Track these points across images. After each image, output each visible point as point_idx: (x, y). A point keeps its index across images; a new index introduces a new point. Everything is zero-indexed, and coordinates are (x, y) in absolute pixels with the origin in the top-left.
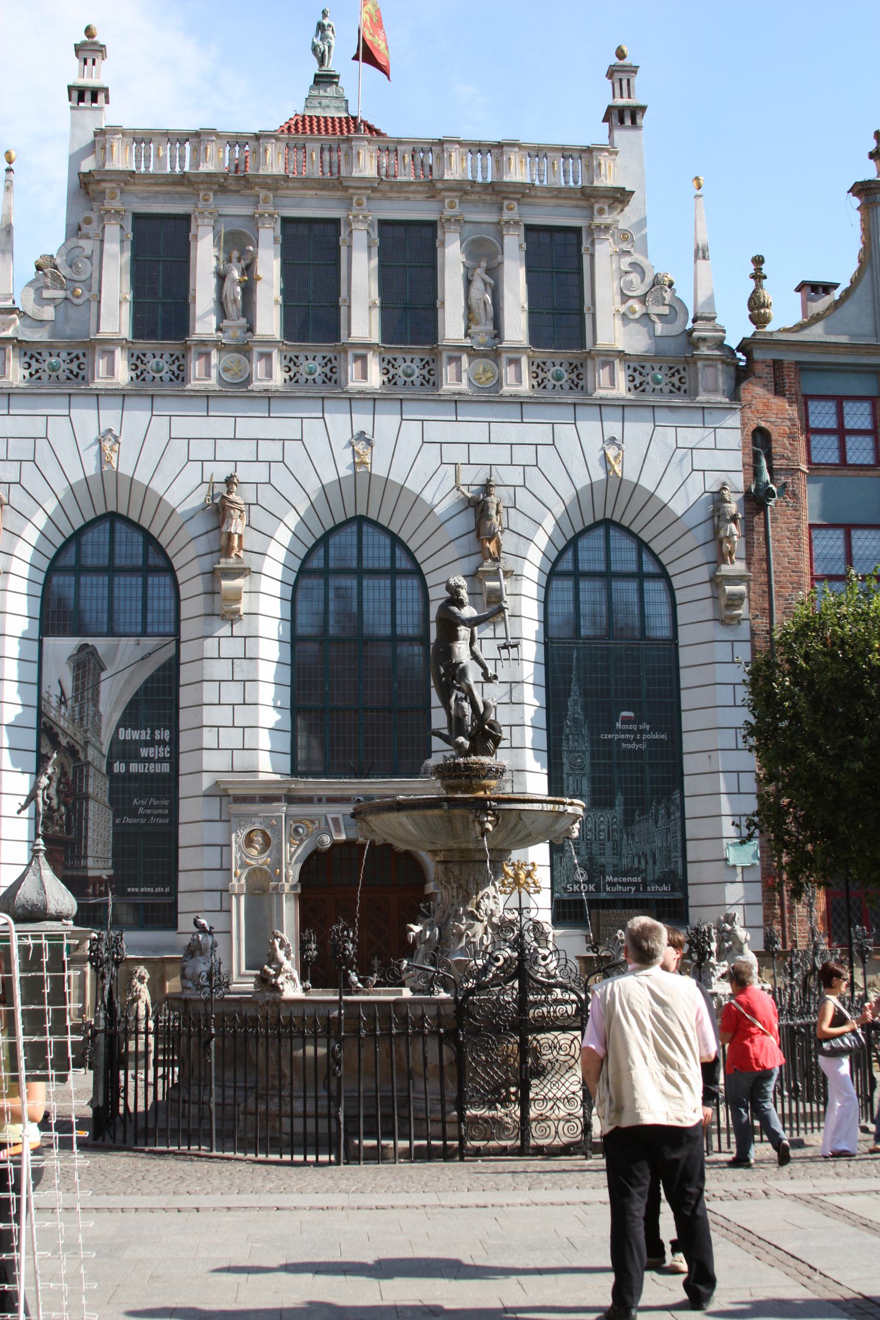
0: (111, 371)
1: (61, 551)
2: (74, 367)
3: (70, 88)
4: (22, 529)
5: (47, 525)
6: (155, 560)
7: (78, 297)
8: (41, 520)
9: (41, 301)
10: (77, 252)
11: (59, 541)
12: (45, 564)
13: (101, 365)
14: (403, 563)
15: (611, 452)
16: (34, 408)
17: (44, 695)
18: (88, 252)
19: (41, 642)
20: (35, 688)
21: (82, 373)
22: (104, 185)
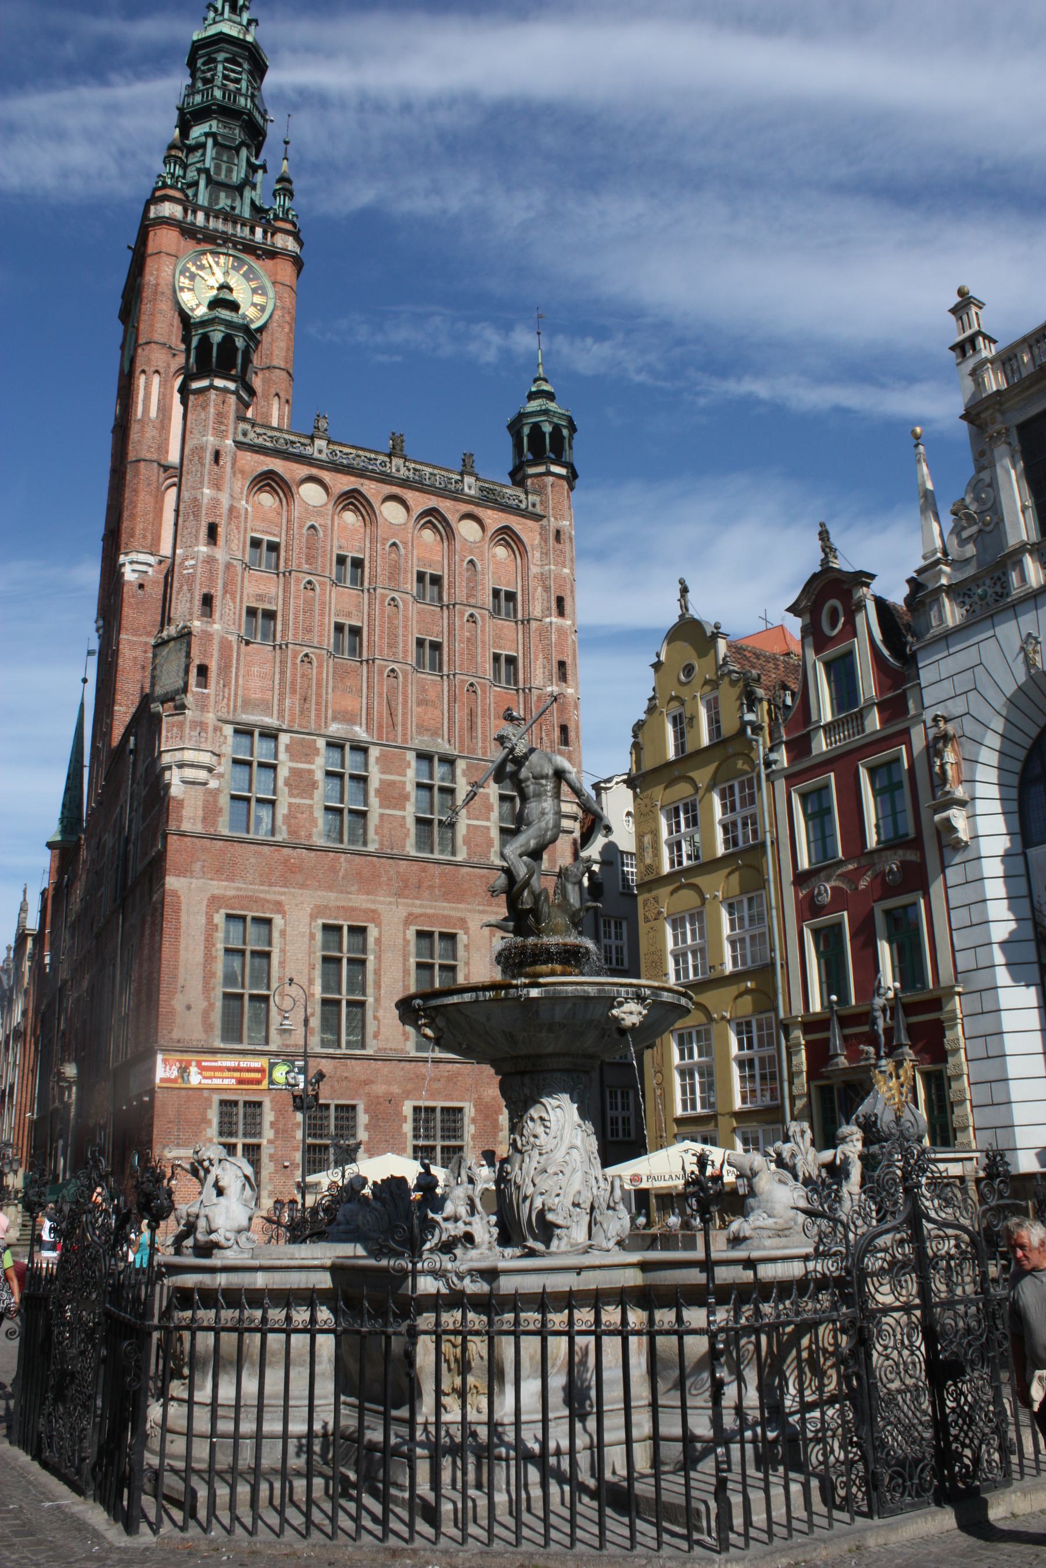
0: (1023, 578)
1: (1027, 763)
2: (998, 589)
3: (952, 348)
4: (978, 754)
5: (1002, 743)
7: (988, 524)
8: (995, 741)
9: (962, 543)
10: (980, 485)
11: (1022, 754)
12: (1015, 780)
13: (1014, 576)
16: (967, 640)
17: (1036, 905)
18: (987, 480)
19: (1025, 854)
20: (1027, 901)
22: (983, 416)
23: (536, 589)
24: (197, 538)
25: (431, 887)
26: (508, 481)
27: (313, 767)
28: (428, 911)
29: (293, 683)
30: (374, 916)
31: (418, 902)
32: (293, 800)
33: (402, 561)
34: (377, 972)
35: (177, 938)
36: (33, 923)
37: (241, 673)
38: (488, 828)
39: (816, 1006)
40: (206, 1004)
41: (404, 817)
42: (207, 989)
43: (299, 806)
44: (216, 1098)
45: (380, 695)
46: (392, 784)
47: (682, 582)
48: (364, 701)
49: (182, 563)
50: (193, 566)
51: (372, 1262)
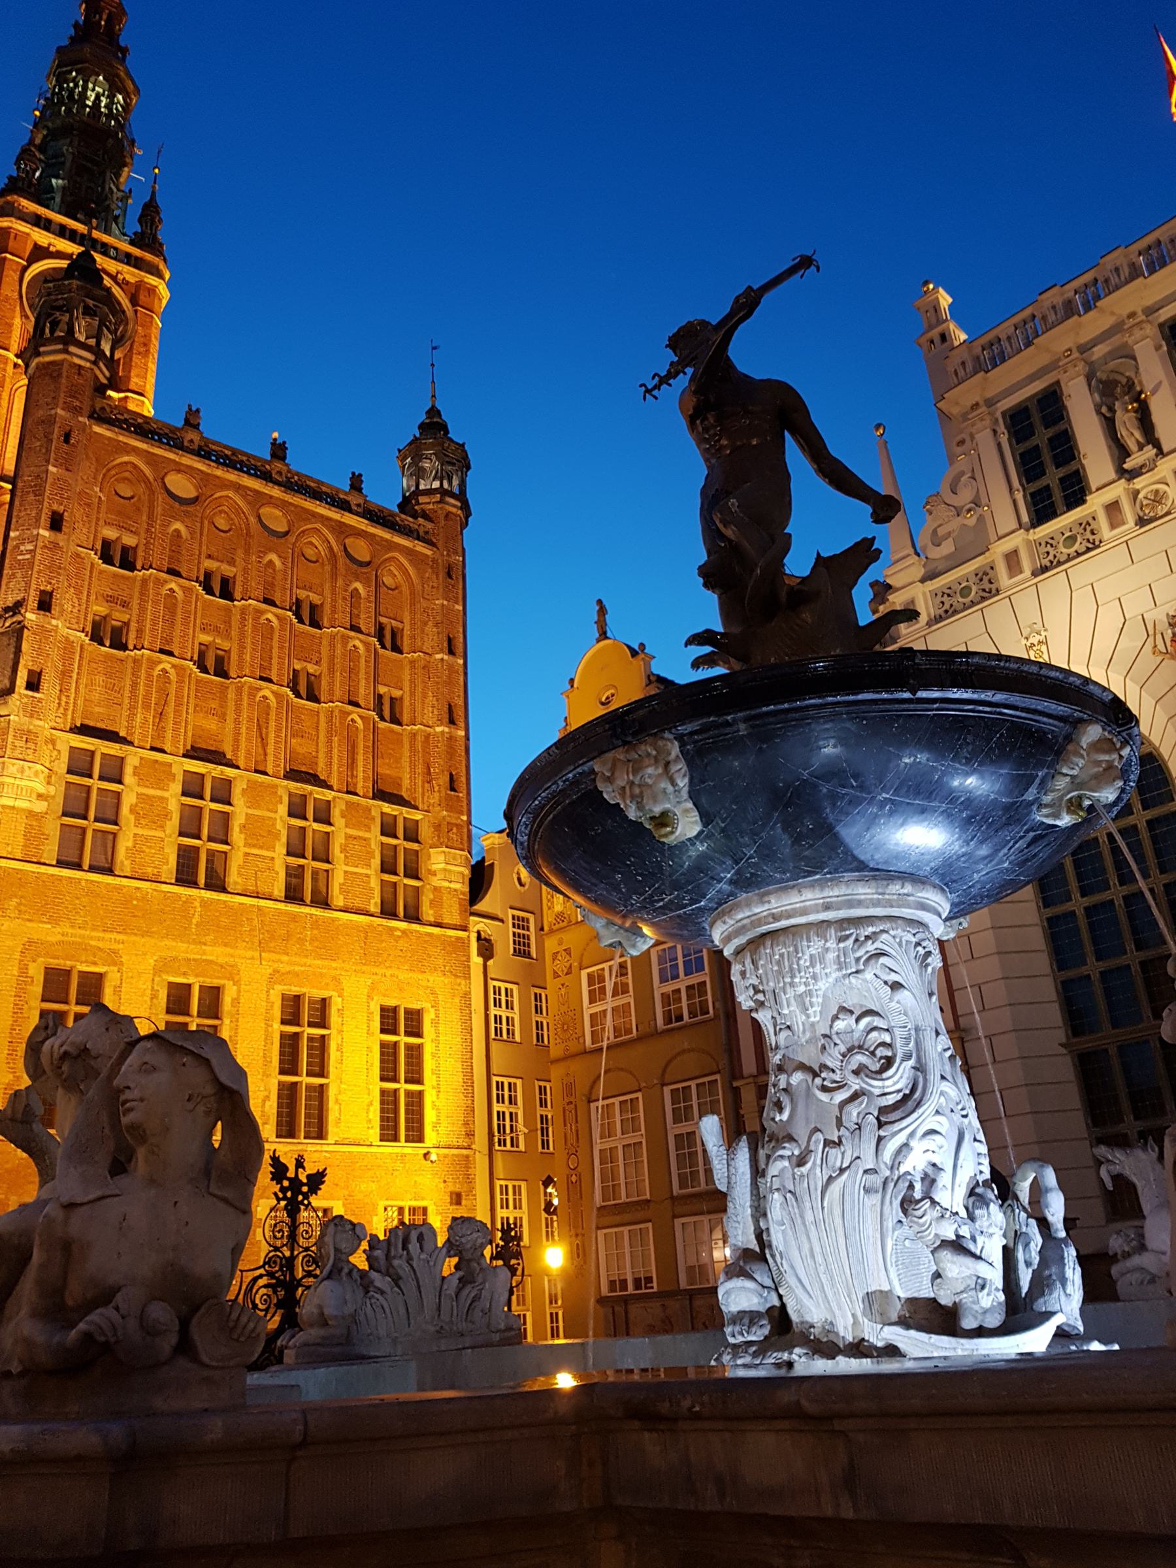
21: (993, 587)
23: (426, 624)
24: (38, 520)
25: (301, 941)
26: (397, 510)
27: (166, 794)
28: (297, 968)
29: (147, 696)
30: (232, 974)
31: (285, 958)
32: (140, 831)
33: (279, 577)
37: (84, 680)
38: (368, 876)
40: (11, 1076)
41: (273, 859)
43: (147, 838)
45: (250, 719)
47: (600, 602)
48: (230, 725)
49: (17, 546)
50: (30, 552)
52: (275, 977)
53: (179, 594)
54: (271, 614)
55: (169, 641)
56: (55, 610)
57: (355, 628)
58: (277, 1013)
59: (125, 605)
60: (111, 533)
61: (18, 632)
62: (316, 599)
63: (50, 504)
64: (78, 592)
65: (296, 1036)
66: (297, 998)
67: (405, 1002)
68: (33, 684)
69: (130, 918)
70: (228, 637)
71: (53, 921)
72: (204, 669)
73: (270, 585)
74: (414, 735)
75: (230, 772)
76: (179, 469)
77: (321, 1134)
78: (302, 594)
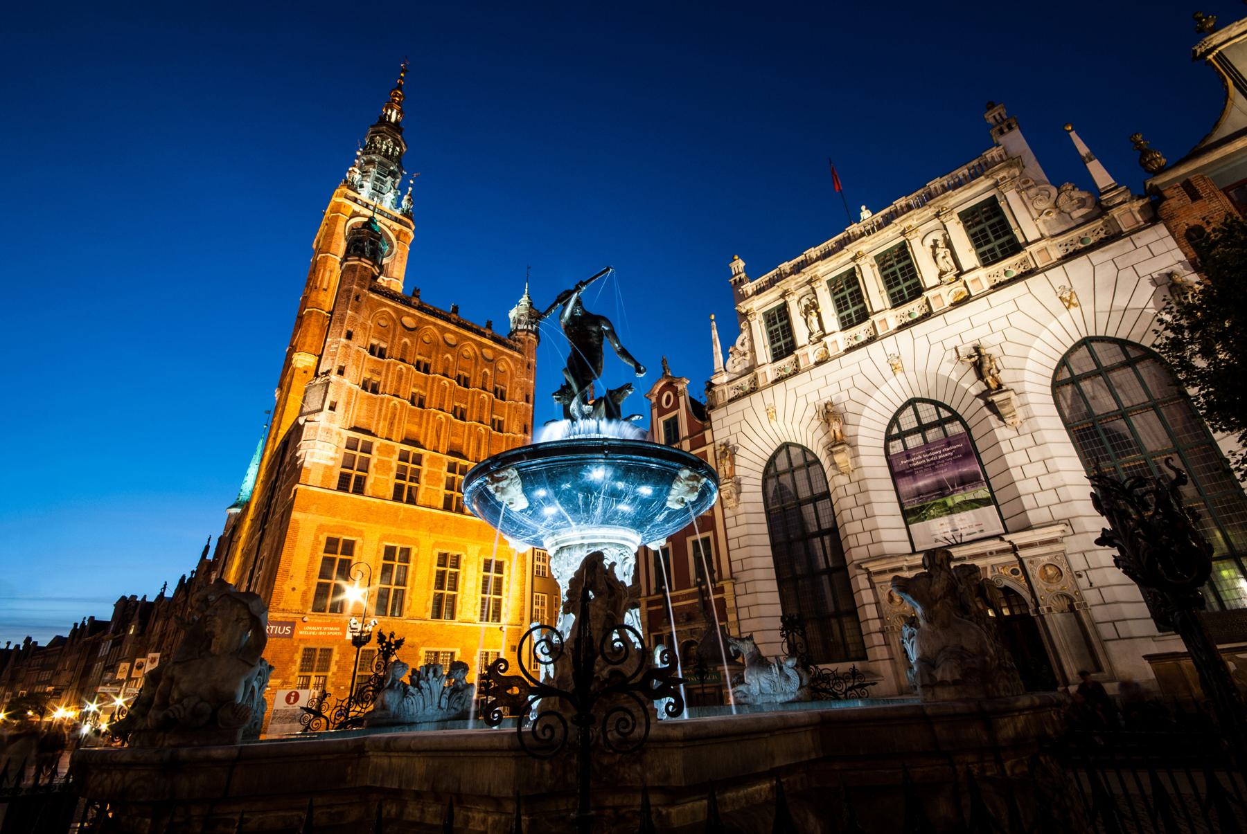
6: (810, 458)
14: (945, 414)
15: (1067, 295)
30: (417, 543)
34: (414, 573)
35: (293, 548)
36: (210, 556)
39: (652, 592)
42: (307, 578)
44: (302, 646)
46: (434, 473)
48: (423, 430)
51: (441, 733)
52: (436, 545)
53: (404, 370)
54: (446, 381)
55: (398, 390)
56: (346, 374)
57: (484, 389)
58: (436, 561)
59: (379, 374)
60: (375, 342)
61: (327, 384)
62: (467, 375)
63: (347, 327)
64: (357, 367)
65: (444, 572)
66: (446, 555)
67: (494, 558)
68: (332, 408)
69: (369, 515)
70: (425, 389)
71: (334, 515)
72: (413, 404)
73: (446, 369)
74: (508, 438)
75: (421, 451)
76: (408, 315)
77: (452, 618)
78: (461, 373)
